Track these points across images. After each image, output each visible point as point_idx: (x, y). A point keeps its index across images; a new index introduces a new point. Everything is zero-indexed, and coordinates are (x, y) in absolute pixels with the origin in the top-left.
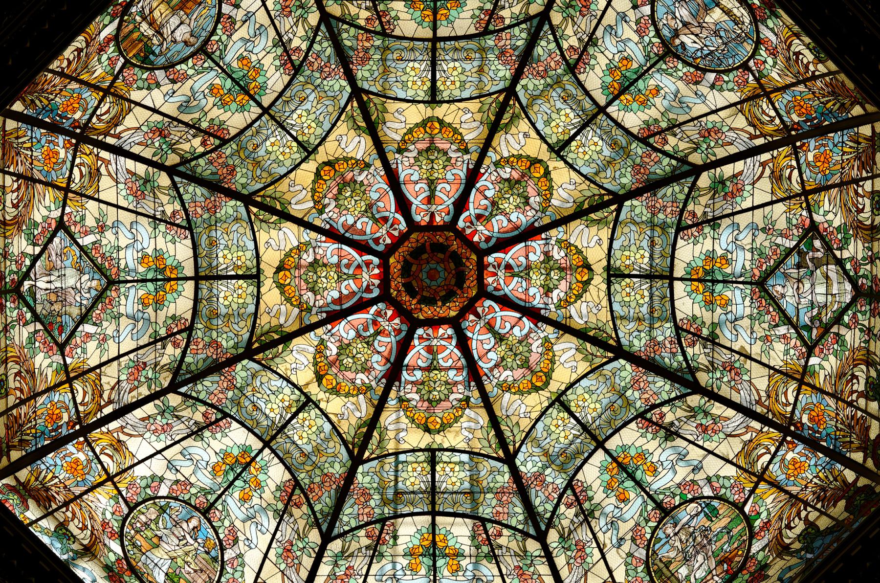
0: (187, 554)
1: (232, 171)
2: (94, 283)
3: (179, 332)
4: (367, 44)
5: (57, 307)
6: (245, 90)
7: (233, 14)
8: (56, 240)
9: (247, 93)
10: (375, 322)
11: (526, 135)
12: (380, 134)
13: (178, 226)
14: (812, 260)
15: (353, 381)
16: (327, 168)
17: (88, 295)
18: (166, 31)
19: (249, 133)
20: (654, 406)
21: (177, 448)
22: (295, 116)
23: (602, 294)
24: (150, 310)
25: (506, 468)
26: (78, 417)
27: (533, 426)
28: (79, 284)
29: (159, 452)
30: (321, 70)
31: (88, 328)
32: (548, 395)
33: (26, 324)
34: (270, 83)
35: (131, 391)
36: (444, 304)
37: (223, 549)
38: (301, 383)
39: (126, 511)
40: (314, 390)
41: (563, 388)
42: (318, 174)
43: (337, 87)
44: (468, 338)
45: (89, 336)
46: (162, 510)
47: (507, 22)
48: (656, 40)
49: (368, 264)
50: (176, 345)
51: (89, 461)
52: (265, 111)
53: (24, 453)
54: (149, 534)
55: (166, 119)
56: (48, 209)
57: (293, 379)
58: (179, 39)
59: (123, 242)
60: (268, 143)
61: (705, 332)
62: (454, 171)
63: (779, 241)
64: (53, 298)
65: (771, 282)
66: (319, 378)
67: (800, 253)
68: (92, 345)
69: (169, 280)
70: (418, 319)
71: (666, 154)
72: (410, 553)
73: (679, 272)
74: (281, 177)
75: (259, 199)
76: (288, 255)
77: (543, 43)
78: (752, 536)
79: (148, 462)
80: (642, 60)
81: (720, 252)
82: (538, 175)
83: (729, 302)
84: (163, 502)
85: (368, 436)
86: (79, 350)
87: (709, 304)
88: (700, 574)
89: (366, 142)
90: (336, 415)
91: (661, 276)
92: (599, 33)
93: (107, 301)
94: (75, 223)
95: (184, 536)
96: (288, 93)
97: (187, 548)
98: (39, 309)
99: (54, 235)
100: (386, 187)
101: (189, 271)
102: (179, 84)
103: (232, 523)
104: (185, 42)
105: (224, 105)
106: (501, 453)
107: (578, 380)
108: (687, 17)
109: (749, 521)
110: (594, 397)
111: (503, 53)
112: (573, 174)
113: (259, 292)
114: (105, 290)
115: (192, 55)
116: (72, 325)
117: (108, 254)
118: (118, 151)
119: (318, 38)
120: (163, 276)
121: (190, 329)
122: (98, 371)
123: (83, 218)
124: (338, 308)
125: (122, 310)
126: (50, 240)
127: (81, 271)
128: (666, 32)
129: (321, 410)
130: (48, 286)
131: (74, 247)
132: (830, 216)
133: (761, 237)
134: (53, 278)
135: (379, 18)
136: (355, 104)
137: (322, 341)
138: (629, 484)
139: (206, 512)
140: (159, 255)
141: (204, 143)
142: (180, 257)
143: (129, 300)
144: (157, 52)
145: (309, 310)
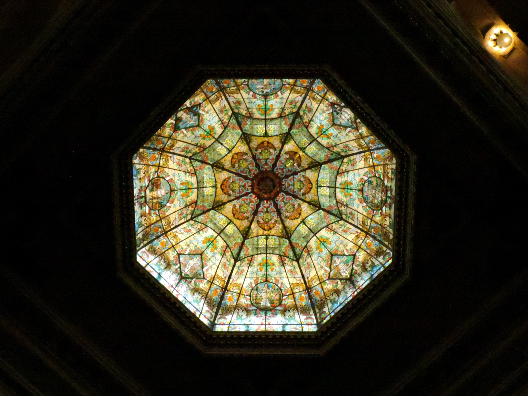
5: (194, 272)
8: (181, 259)
11: (256, 139)
14: (339, 110)
15: (272, 223)
18: (160, 196)
20: (339, 169)
24: (215, 251)
25: (321, 211)
28: (194, 263)
30: (200, 168)
31: (205, 269)
33: (191, 282)
34: (193, 182)
37: (277, 285)
38: (262, 234)
39: (249, 297)
40: (266, 233)
46: (257, 289)
49: (251, 196)
51: (232, 295)
56: (173, 254)
59: (196, 244)
61: (334, 144)
63: (328, 112)
64: (192, 270)
65: (335, 122)
66: (264, 229)
67: (335, 111)
68: (210, 271)
73: (316, 137)
76: (233, 211)
78: (383, 181)
80: (262, 102)
81: (319, 125)
83: (331, 134)
84: (255, 288)
87: (328, 137)
88: (380, 199)
91: (313, 140)
92: (248, 105)
98: (191, 276)
99: (179, 258)
101: (216, 235)
104: (166, 193)
105: (188, 196)
106: (317, 208)
108: (262, 86)
109: (379, 178)
111: (233, 128)
112: (274, 137)
115: (171, 194)
116: (201, 272)
118: (176, 227)
120: (211, 242)
121: (228, 246)
123: (182, 248)
125: (209, 257)
126: (179, 260)
127: (192, 259)
128: (261, 93)
132: (333, 99)
133: (324, 114)
137: (258, 221)
138: (349, 191)
139: (266, 281)
140: (206, 238)
141: (192, 207)
142: (211, 234)
143: (208, 253)
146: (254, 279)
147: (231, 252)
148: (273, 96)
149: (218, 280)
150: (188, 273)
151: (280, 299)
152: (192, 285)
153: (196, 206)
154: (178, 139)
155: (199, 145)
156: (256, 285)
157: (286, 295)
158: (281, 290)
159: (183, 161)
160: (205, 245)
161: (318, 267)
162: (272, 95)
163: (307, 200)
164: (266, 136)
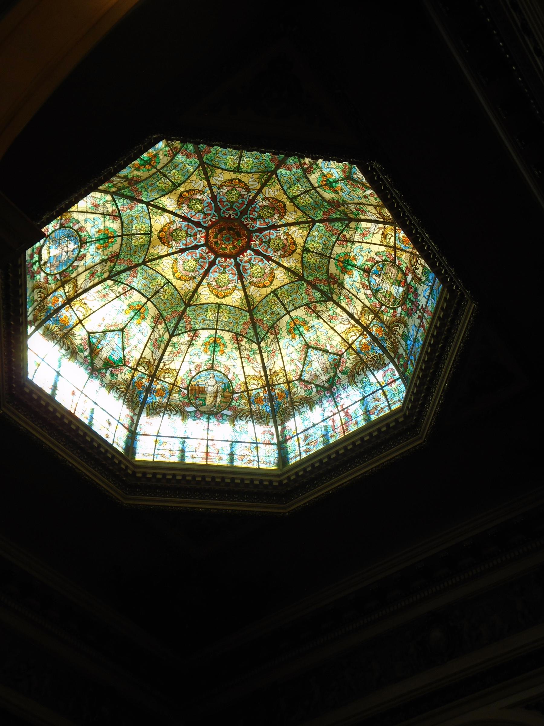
0: (387, 278)
1: (245, 323)
2: (312, 353)
3: (311, 308)
4: (169, 316)
6: (215, 342)
7: (193, 369)
8: (306, 378)
9: (215, 340)
10: (260, 244)
12: (194, 288)
13: (275, 331)
16: (219, 296)
17: (318, 354)
19: (228, 329)
21: (351, 290)
22: (211, 318)
23: (186, 184)
26: (361, 334)
27: (255, 172)
29: (356, 297)
31: (328, 348)
32: (239, 176)
33: (339, 378)
34: (207, 336)
35: (341, 316)
36: (235, 229)
37: (378, 262)
40: (299, 250)
41: (232, 173)
42: (224, 297)
43: (191, 313)
44: (241, 212)
45: (331, 347)
47: (122, 286)
48: (82, 250)
50: (316, 307)
52: (216, 329)
53: (384, 355)
54: (388, 296)
55: (243, 360)
57: (300, 259)
58: (214, 381)
60: (226, 320)
62: (187, 257)
68: (334, 343)
69: (295, 323)
70: (247, 233)
71: (117, 207)
72: (336, 192)
74: (234, 307)
75: (247, 308)
77: (118, 269)
79: (363, 301)
82: (164, 234)
85: (302, 223)
86: (338, 348)
89: (200, 290)
90: (303, 238)
93: (315, 345)
94: (297, 373)
95: (382, 280)
96: (205, 327)
97: (385, 278)
98: (332, 374)
100: (210, 273)
102: (229, 367)
103: (366, 261)
104: (214, 377)
106: (274, 176)
107: (225, 170)
110: (226, 161)
112: (153, 224)
113: (278, 288)
114: (313, 348)
115: (216, 370)
116: (331, 356)
117: (300, 353)
118: (264, 368)
119: (180, 332)
122: (341, 334)
123: (294, 371)
124: (264, 260)
125: (315, 336)
129: (305, 244)
130: (322, 374)
131: (304, 369)
134: (319, 374)
135: (158, 321)
136: (191, 302)
137: (280, 257)
141: (242, 341)
143: (310, 336)
144: (224, 385)
145: (272, 268)
146: (361, 287)
147: (317, 302)
148: (82, 234)
149: (349, 335)
150: (328, 377)
151: (397, 269)
152: (345, 380)
153: (242, 335)
154: (138, 357)
155: (153, 325)
156: (370, 289)
157: (395, 258)
158: (385, 261)
159: (174, 347)
160: (297, 337)
161: (364, 201)
162: (80, 236)
163: (258, 188)
164: (150, 234)
